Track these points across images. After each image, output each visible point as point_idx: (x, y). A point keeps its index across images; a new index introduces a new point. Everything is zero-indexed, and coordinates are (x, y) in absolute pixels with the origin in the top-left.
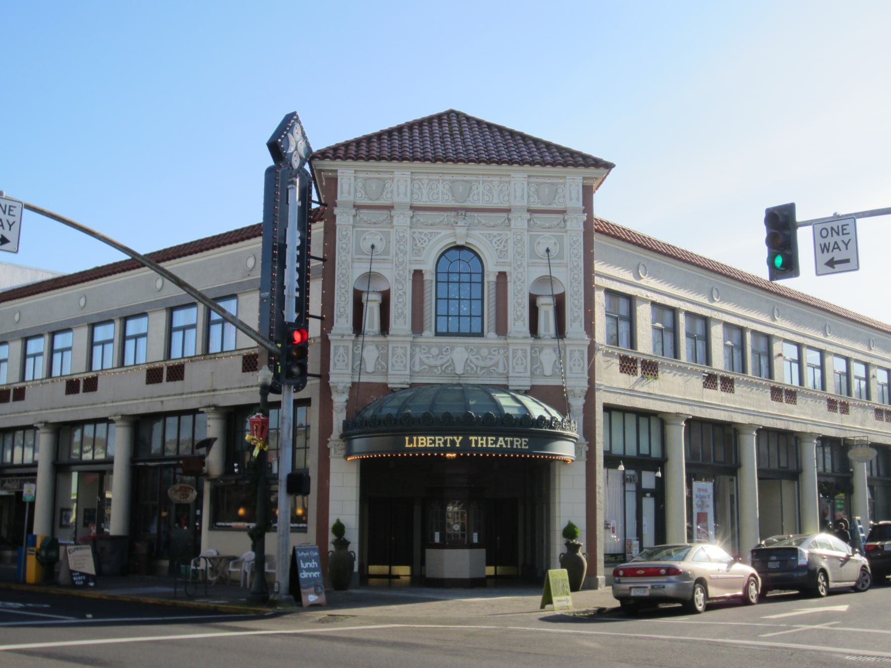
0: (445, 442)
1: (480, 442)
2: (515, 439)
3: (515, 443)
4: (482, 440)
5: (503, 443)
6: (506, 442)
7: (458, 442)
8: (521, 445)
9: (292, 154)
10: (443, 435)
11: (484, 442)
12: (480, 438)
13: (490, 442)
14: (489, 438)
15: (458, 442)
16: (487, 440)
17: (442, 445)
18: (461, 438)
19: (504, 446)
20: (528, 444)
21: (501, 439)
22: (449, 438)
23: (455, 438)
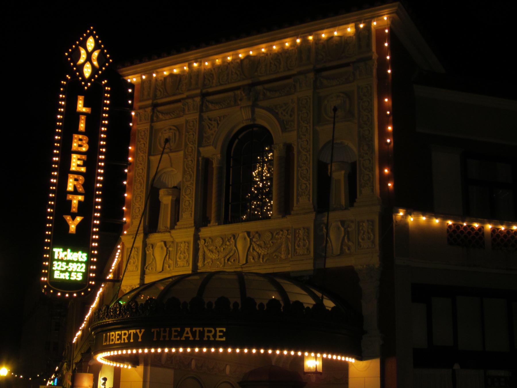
0: (129, 338)
1: (162, 334)
2: (206, 329)
3: (206, 334)
4: (165, 331)
5: (190, 335)
6: (194, 334)
7: (140, 335)
8: (215, 336)
9: (83, 65)
10: (128, 328)
11: (167, 334)
12: (162, 329)
13: (174, 334)
14: (173, 329)
15: (140, 335)
16: (170, 332)
17: (126, 341)
18: (143, 330)
19: (191, 338)
20: (225, 334)
21: (188, 329)
22: (132, 331)
23: (138, 331)
